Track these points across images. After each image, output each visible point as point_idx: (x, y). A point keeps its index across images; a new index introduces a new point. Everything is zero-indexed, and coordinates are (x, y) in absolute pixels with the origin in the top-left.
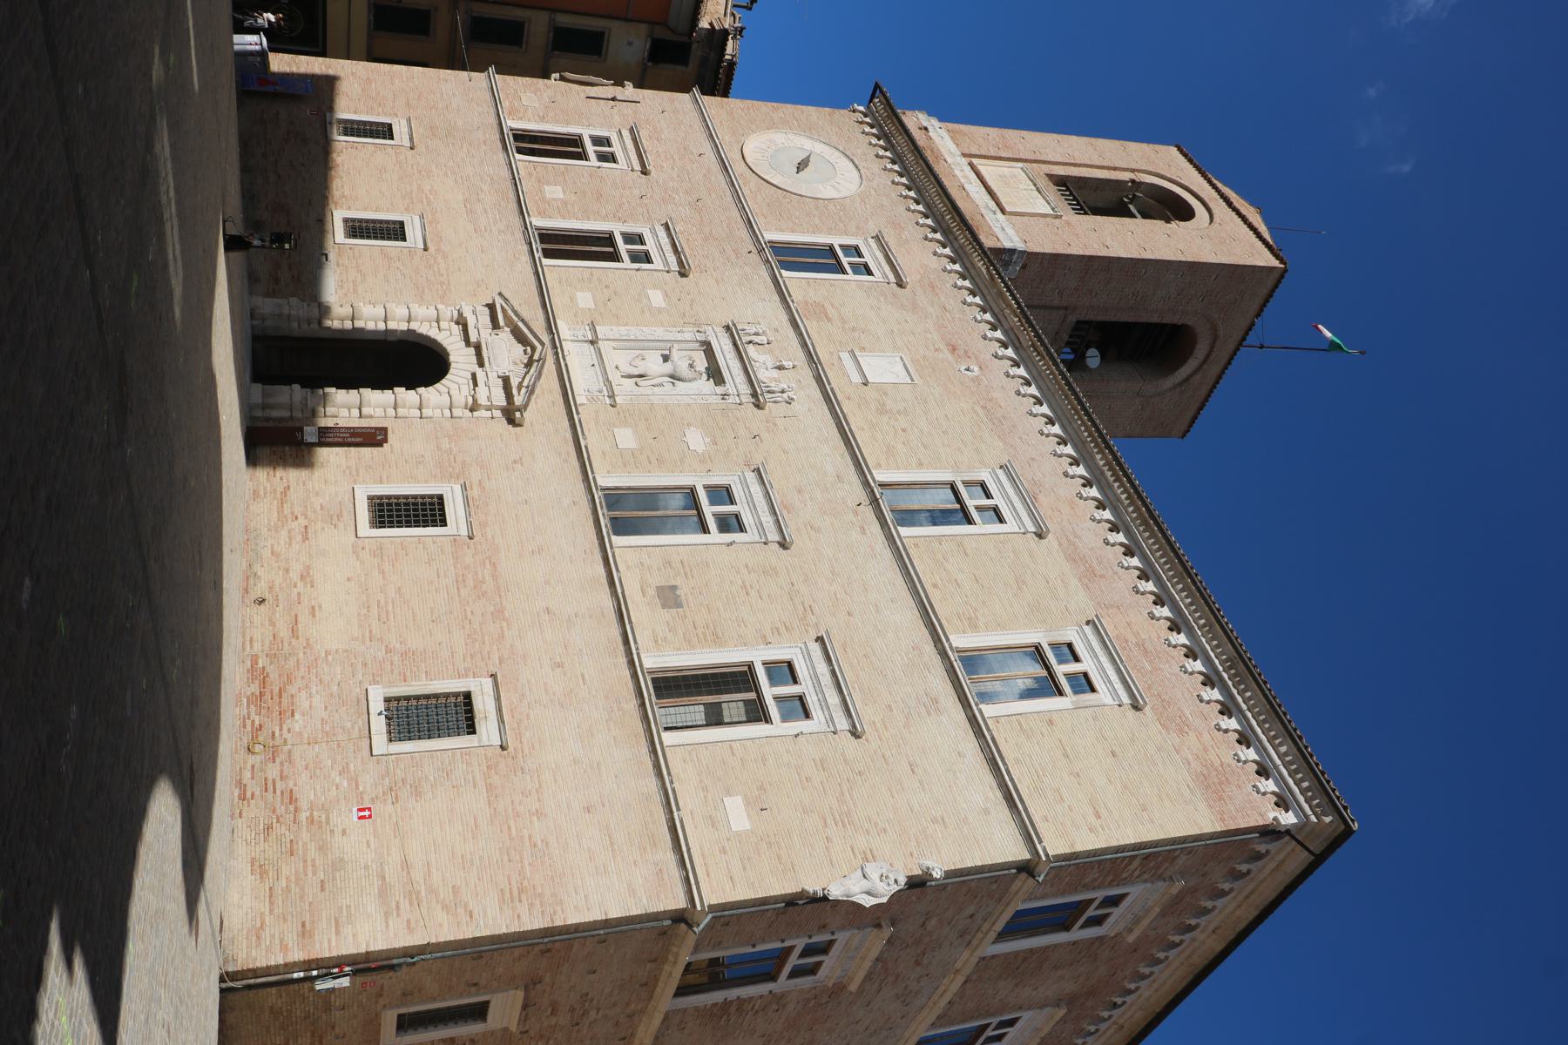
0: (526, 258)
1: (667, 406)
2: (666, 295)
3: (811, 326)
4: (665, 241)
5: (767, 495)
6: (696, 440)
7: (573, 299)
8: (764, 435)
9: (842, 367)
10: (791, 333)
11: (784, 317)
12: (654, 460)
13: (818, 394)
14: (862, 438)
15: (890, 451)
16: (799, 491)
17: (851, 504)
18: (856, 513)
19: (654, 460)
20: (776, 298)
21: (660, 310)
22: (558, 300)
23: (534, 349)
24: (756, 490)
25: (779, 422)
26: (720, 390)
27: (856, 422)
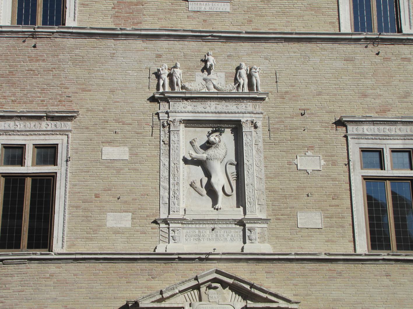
0: (52, 268)
1: (267, 177)
2: (110, 143)
3: (150, 24)
4: (20, 125)
5: (374, 123)
6: (310, 162)
7: (117, 232)
8: (301, 104)
9: (211, 14)
10: (163, 44)
11: (139, 44)
12: (334, 202)
13: (247, 46)
14: (299, 27)
15: (315, 9)
16: (365, 96)
17: (378, 59)
18: (386, 59)
19: (334, 202)
20: (111, 42)
21: (131, 154)
22: (121, 246)
23: (215, 280)
24: (366, 129)
25: (283, 88)
26: (246, 128)
27: (280, 26)
